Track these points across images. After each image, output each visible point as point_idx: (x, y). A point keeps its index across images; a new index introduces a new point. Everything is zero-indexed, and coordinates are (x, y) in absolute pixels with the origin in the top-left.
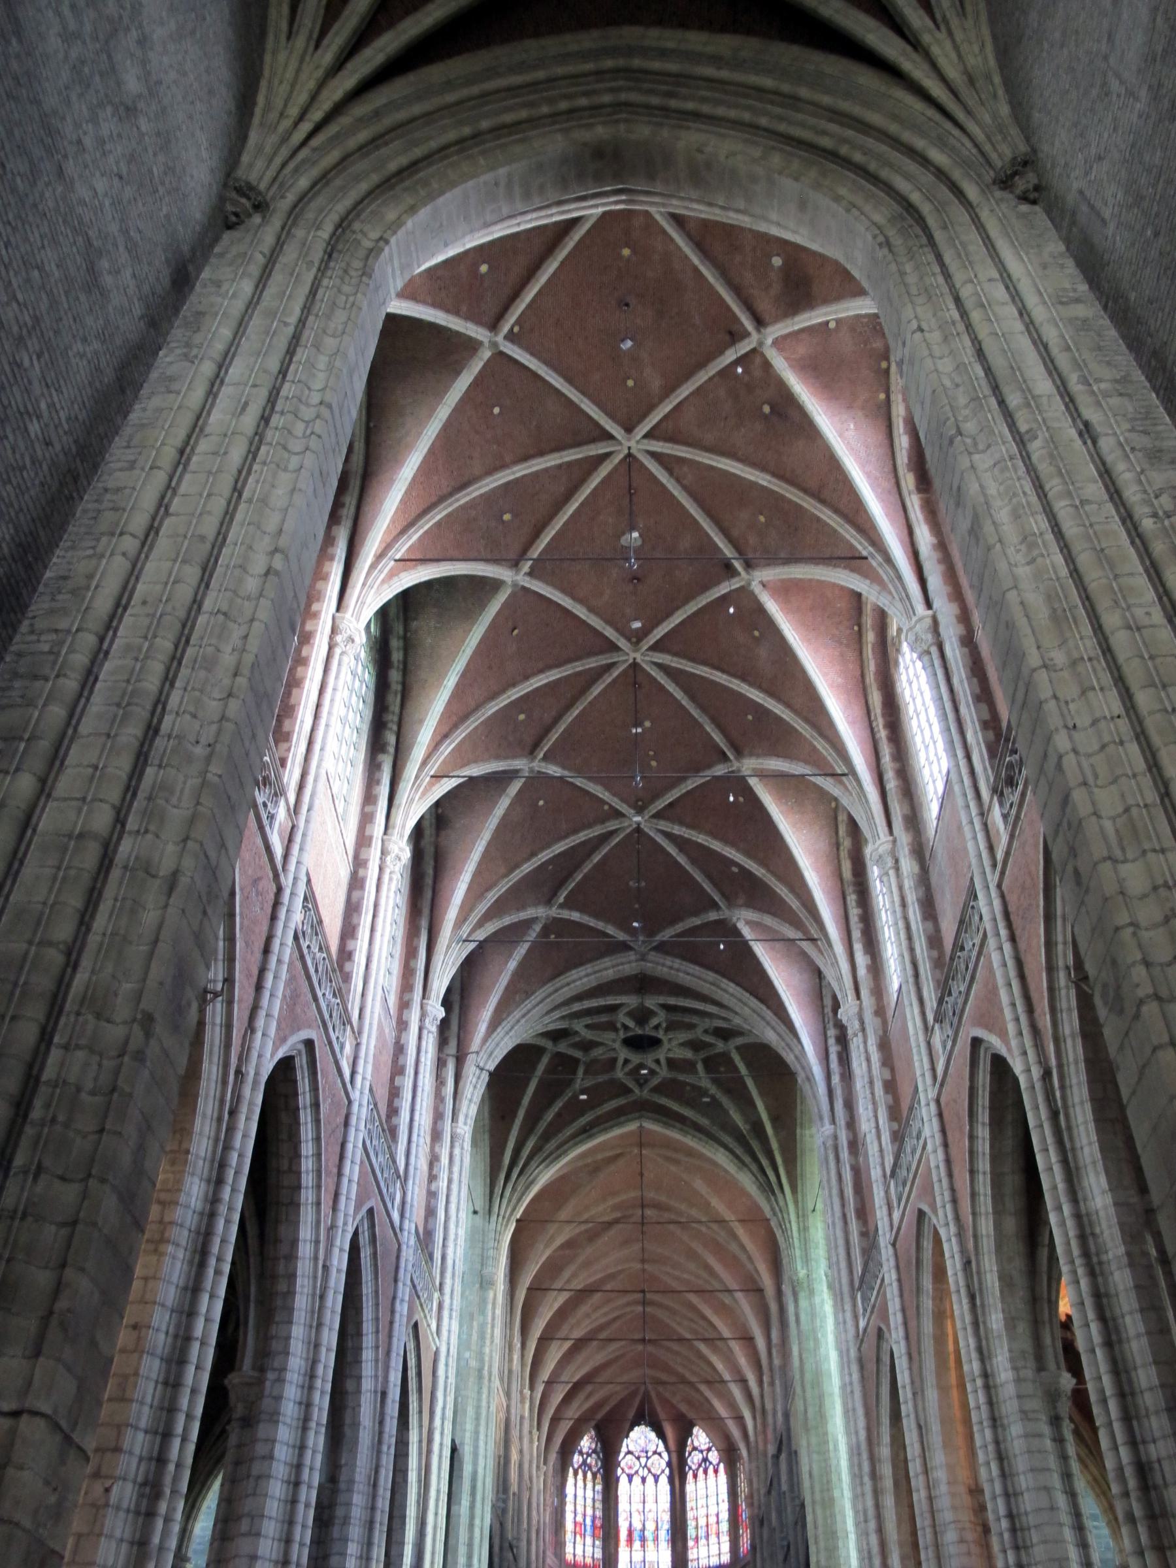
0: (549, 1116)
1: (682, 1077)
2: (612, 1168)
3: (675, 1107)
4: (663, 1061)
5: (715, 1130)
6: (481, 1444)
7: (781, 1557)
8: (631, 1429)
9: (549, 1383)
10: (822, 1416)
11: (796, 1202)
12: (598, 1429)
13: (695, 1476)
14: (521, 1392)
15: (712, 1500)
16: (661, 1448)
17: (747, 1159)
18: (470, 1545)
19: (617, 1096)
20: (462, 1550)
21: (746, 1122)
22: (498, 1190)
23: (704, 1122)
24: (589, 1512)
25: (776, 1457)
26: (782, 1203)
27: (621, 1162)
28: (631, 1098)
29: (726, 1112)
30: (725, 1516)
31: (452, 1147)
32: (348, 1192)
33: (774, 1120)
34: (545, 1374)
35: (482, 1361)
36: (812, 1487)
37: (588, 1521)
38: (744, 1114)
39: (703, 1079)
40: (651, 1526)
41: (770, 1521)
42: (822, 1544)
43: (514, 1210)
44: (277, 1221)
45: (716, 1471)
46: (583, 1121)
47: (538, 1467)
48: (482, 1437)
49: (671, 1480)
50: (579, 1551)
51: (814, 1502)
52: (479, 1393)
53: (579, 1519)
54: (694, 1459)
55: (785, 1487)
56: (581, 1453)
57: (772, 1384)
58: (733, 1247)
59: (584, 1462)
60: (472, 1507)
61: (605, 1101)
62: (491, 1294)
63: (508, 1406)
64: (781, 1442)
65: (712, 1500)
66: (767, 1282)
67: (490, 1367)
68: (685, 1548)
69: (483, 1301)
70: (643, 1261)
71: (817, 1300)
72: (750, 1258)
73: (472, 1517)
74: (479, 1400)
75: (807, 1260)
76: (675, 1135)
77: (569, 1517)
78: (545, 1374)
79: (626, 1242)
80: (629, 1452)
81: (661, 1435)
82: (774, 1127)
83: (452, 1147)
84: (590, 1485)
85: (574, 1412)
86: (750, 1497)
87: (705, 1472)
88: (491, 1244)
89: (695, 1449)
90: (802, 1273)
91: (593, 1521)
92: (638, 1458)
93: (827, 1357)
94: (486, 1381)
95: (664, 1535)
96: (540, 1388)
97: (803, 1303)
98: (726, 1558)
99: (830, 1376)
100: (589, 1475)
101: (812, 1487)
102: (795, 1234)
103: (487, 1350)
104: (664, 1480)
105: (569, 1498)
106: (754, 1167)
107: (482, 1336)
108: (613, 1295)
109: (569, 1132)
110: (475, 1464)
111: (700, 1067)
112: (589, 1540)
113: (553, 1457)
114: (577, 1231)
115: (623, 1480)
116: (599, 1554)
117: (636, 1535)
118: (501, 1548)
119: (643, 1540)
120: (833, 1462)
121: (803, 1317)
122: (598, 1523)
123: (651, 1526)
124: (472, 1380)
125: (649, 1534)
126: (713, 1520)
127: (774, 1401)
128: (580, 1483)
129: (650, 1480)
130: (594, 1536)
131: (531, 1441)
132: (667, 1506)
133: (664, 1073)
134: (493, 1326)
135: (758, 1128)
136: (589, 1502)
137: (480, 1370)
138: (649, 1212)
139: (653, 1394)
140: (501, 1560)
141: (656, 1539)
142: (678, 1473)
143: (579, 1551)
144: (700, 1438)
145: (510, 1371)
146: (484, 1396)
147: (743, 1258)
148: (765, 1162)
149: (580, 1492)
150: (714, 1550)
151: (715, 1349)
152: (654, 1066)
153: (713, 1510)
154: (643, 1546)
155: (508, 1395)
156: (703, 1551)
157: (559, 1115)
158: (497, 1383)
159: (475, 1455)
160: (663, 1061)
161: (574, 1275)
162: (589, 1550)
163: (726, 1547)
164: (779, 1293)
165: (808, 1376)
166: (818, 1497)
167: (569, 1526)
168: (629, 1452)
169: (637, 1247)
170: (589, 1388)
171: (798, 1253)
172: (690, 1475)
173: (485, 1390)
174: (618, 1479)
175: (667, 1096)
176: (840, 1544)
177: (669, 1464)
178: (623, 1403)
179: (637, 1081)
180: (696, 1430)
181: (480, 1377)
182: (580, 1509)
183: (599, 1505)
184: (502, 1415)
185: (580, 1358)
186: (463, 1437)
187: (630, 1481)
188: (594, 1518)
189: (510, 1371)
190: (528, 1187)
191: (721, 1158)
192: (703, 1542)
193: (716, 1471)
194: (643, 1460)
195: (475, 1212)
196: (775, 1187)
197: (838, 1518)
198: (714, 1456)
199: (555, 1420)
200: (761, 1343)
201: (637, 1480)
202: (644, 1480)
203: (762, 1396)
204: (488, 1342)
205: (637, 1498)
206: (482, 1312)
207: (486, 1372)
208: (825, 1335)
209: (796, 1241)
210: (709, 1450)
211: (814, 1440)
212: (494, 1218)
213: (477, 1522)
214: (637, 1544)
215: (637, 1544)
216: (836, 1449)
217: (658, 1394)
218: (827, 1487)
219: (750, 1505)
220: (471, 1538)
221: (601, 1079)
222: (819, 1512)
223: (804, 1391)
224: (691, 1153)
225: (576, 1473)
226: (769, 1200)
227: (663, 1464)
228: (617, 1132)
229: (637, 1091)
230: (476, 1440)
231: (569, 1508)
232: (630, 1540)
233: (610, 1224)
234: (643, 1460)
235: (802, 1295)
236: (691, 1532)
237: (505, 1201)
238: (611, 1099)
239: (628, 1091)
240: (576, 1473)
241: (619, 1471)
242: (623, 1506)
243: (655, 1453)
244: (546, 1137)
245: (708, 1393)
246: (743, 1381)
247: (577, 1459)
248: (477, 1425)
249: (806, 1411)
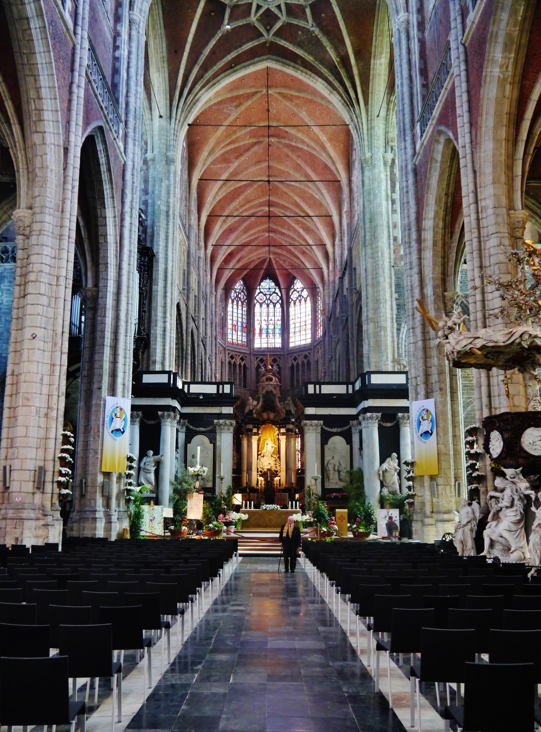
0: (207, 51)
1: (295, 22)
2: (249, 102)
3: (291, 47)
4: (283, 7)
5: (316, 64)
6: (170, 253)
7: (341, 328)
8: (262, 281)
9: (217, 246)
10: (374, 237)
11: (367, 111)
12: (243, 279)
13: (295, 303)
14: (198, 244)
15: (303, 315)
16: (277, 291)
17: (337, 84)
18: (165, 307)
19: (252, 40)
20: (160, 310)
21: (338, 55)
22: (175, 103)
23: (309, 58)
24: (240, 320)
25: (341, 279)
26: (357, 111)
27: (255, 98)
28: (262, 40)
29: (323, 48)
30: (309, 322)
31: (130, 29)
33: (357, 54)
34: (212, 241)
35: (168, 206)
36: (366, 277)
37: (239, 324)
38: (336, 49)
39: (310, 24)
40: (271, 327)
41: (335, 315)
42: (371, 306)
43: (186, 117)
45: (305, 301)
46: (229, 57)
47: (211, 293)
48: (170, 249)
49: (282, 306)
50: (235, 337)
51: (367, 285)
52: (167, 224)
53: (235, 323)
54: (294, 296)
55: (345, 293)
56: (236, 292)
57: (341, 240)
58: (324, 157)
59: (237, 296)
60: (165, 287)
61: (244, 43)
62: (172, 168)
63: (189, 247)
64: (345, 269)
65: (303, 315)
66: (343, 176)
67: (174, 210)
68: (288, 337)
69: (169, 172)
70: (269, 176)
71: (376, 171)
72: (333, 162)
73: (165, 292)
74: (167, 229)
75: (371, 148)
76: (290, 71)
77: (230, 322)
79: (259, 162)
80: (261, 292)
81: (277, 284)
82: (357, 59)
83: (130, 29)
84: (240, 308)
86: (324, 310)
87: (300, 301)
88: (172, 137)
89: (295, 290)
90: (368, 155)
91: (242, 325)
92: (265, 295)
93: (380, 205)
94: (171, 218)
95: (278, 331)
96: (210, 249)
97: (367, 173)
98: (309, 341)
99: (382, 215)
100: (240, 303)
101: (366, 277)
102: (365, 131)
103: (171, 200)
104: (278, 306)
105: (229, 313)
106: (341, 89)
107: (168, 193)
108: (254, 248)
109: (221, 64)
110: (166, 264)
111: (308, 11)
112: (240, 333)
113: (220, 291)
114: (229, 148)
115: (258, 306)
116: (245, 339)
117: (264, 332)
118: (187, 318)
119: (267, 333)
120: (381, 263)
121: (367, 181)
122: (244, 325)
123: (271, 327)
124: (163, 217)
125: (271, 331)
126: (303, 324)
127: (342, 248)
128: (235, 307)
129: (271, 306)
130: (242, 331)
131: (206, 276)
132: (280, 318)
133: (283, 18)
134: (175, 188)
135: (345, 61)
136: (240, 316)
137: (167, 212)
138: (273, 140)
139: (274, 262)
140: (187, 323)
141: (274, 333)
142: (285, 303)
143: (235, 337)
144: (298, 285)
145: (190, 225)
146: (171, 226)
147: (330, 164)
148: (348, 84)
149: (235, 311)
150: (303, 337)
151: (308, 230)
152: (276, 11)
153: (303, 319)
154: (267, 336)
155: (188, 238)
156: (298, 338)
157: (212, 52)
158: (178, 221)
159: (166, 259)
160: (283, 7)
161: (237, 238)
162: (240, 338)
163: (309, 336)
164: (350, 181)
165: (367, 216)
166: (370, 281)
167: (230, 326)
168: (261, 292)
169: (265, 164)
170: (239, 256)
171: (366, 143)
172: (292, 303)
173: (171, 223)
174: (255, 305)
175: (286, 40)
176: (381, 306)
177: (281, 298)
178: (257, 268)
179: (265, 28)
180: (295, 281)
181: (168, 216)
182: (235, 319)
183: (245, 317)
184: (185, 248)
185: (233, 236)
186: (158, 249)
187: (261, 306)
188: (242, 323)
189: (190, 225)
190: (195, 102)
191: (319, 85)
192: (298, 334)
193: (305, 301)
194: (268, 297)
195: (161, 117)
196: (354, 101)
197: (381, 292)
198: (305, 293)
199: (221, 270)
200: (336, 219)
201: (264, 306)
202: (268, 305)
203: (334, 253)
204: (172, 196)
205: (264, 314)
206: (168, 179)
207: (171, 213)
208: (380, 192)
209: (365, 136)
211: (369, 251)
212: (173, 120)
213: (169, 295)
214: (264, 336)
215: (264, 336)
216: (382, 256)
217: (277, 262)
218: (376, 276)
219: (323, 313)
220: (165, 303)
221: (241, 23)
222: (370, 289)
223: (364, 224)
224: (302, 87)
225: (233, 302)
226: (349, 111)
227: (278, 298)
228: (252, 69)
229: (265, 33)
230: (167, 251)
231: (229, 317)
232: (261, 334)
233: (248, 148)
234: (268, 297)
235: (367, 169)
236: (292, 330)
237: (180, 110)
238: (248, 41)
239: (261, 35)
240: (233, 302)
241: (255, 301)
242: (257, 317)
243: (274, 292)
244: (205, 68)
245: (303, 259)
246: (322, 246)
247: (233, 294)
248: (167, 243)
249: (365, 236)
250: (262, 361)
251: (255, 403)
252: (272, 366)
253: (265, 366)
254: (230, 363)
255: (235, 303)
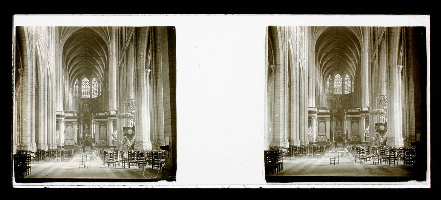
8: (336, 74)
32: (287, 34)
34: (323, 66)
44: (275, 40)
78: (323, 66)
85: (328, 72)
87: (348, 81)
89: (346, 77)
200: (357, 62)
210: (348, 77)
211: (363, 76)
240: (328, 81)
250: (337, 98)
251: (335, 111)
252: (340, 100)
253: (338, 100)
254: (327, 99)
255: (329, 81)
